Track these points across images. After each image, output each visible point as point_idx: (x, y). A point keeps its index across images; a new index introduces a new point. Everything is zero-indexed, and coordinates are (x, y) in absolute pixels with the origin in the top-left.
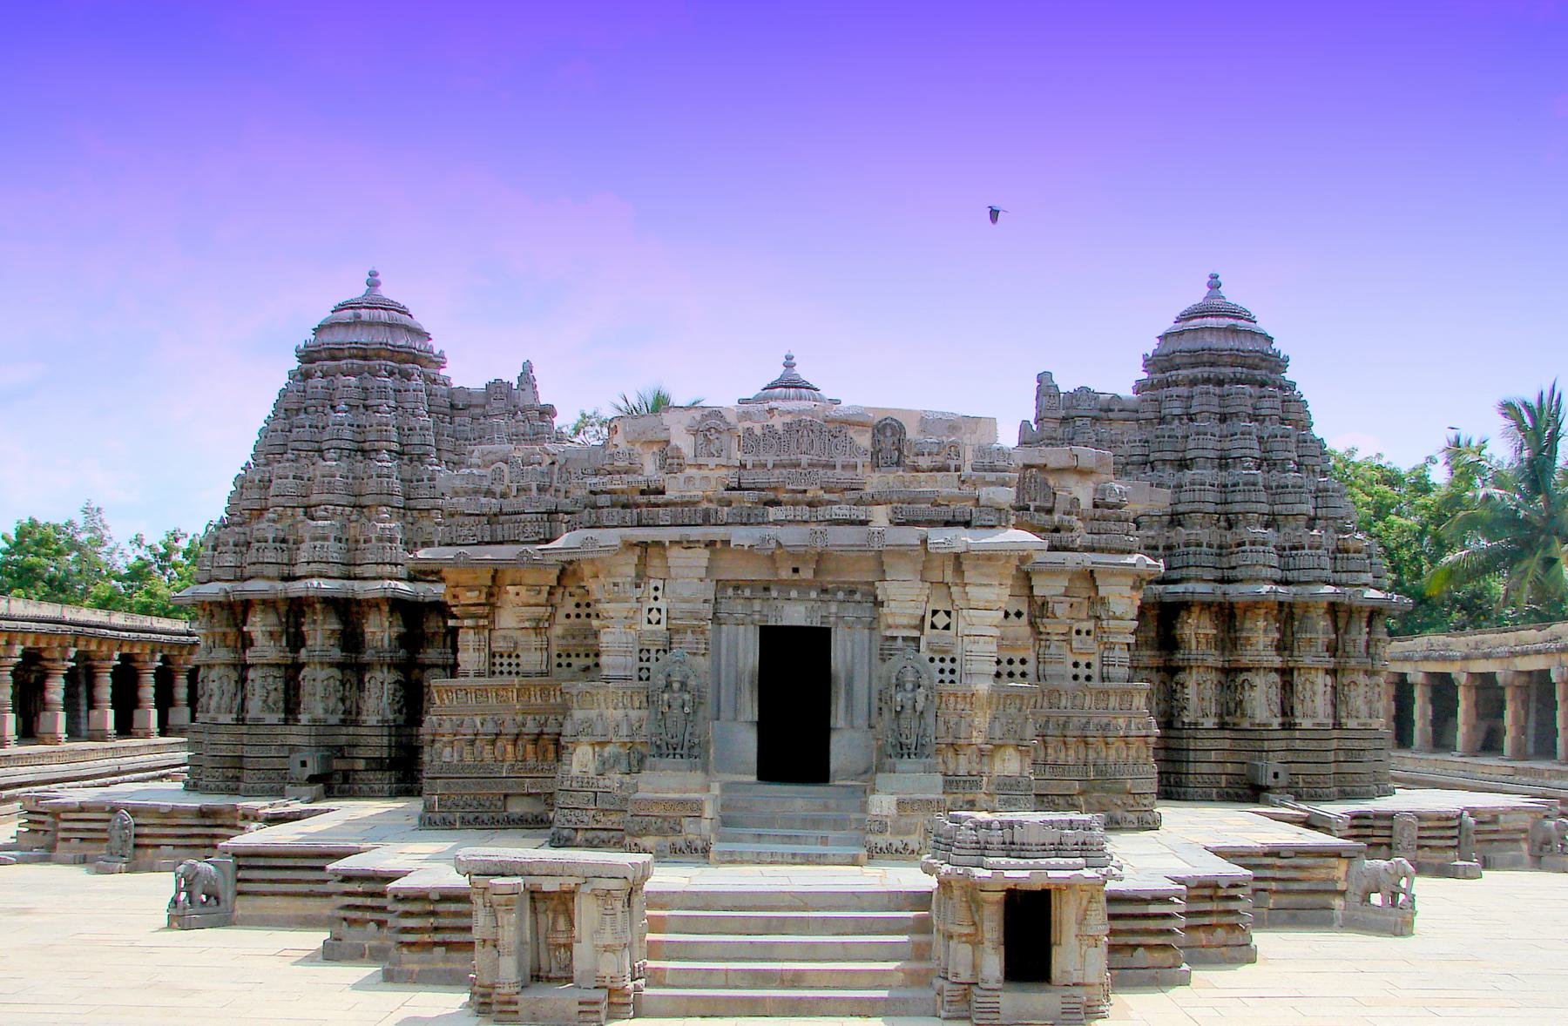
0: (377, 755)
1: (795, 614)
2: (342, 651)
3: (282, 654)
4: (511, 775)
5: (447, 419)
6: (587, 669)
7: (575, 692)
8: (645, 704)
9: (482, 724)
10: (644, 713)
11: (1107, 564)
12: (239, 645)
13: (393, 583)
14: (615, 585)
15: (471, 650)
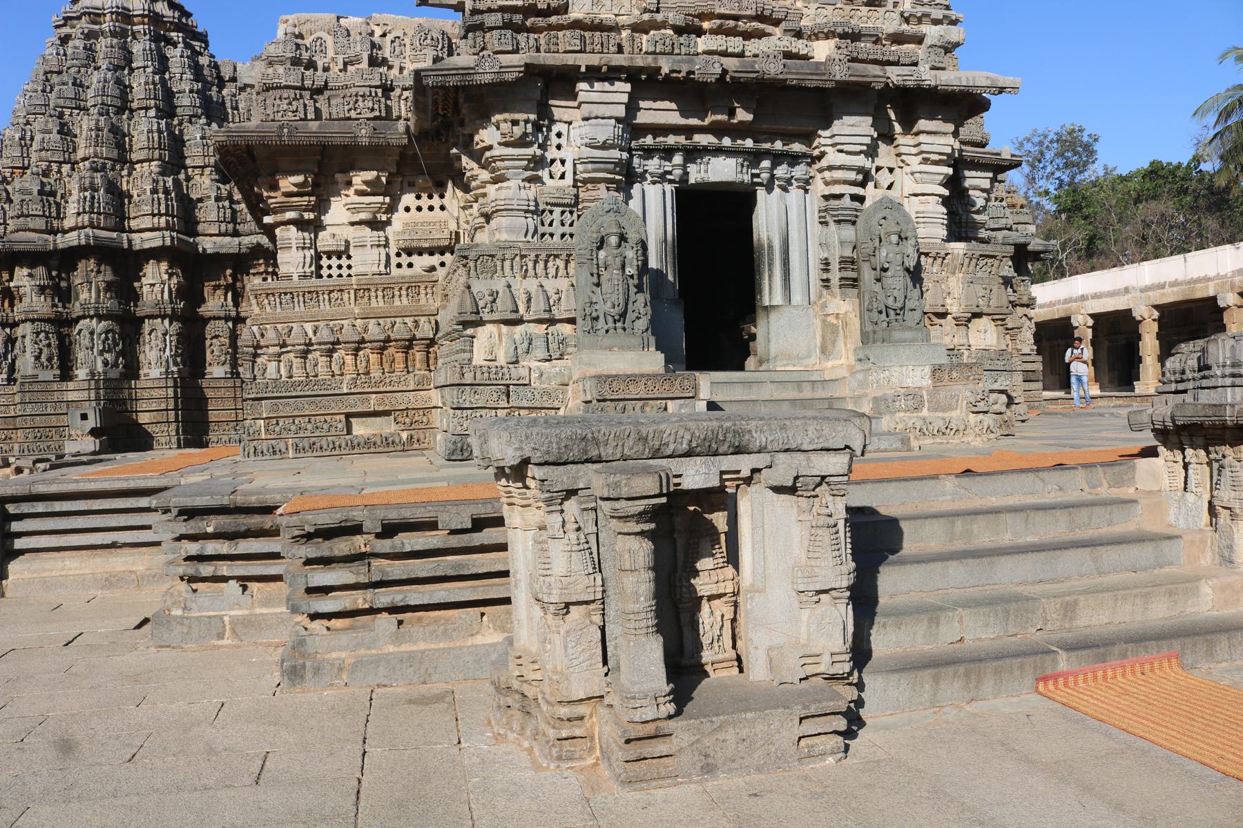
0: (163, 406)
1: (722, 170)
2: (120, 304)
3: (55, 309)
4: (353, 391)
5: (214, 88)
6: (432, 269)
7: (472, 255)
8: (562, 272)
9: (315, 333)
10: (563, 284)
11: (972, 152)
12: (6, 304)
13: (175, 234)
14: (515, 123)
15: (294, 249)
